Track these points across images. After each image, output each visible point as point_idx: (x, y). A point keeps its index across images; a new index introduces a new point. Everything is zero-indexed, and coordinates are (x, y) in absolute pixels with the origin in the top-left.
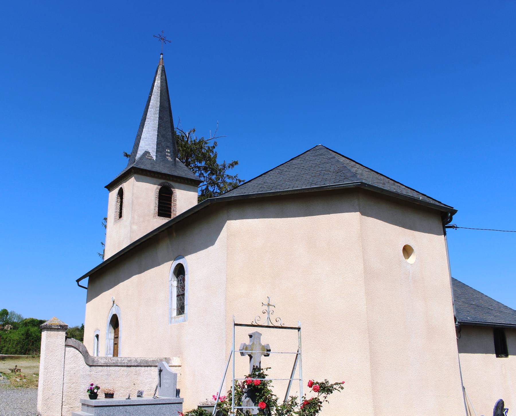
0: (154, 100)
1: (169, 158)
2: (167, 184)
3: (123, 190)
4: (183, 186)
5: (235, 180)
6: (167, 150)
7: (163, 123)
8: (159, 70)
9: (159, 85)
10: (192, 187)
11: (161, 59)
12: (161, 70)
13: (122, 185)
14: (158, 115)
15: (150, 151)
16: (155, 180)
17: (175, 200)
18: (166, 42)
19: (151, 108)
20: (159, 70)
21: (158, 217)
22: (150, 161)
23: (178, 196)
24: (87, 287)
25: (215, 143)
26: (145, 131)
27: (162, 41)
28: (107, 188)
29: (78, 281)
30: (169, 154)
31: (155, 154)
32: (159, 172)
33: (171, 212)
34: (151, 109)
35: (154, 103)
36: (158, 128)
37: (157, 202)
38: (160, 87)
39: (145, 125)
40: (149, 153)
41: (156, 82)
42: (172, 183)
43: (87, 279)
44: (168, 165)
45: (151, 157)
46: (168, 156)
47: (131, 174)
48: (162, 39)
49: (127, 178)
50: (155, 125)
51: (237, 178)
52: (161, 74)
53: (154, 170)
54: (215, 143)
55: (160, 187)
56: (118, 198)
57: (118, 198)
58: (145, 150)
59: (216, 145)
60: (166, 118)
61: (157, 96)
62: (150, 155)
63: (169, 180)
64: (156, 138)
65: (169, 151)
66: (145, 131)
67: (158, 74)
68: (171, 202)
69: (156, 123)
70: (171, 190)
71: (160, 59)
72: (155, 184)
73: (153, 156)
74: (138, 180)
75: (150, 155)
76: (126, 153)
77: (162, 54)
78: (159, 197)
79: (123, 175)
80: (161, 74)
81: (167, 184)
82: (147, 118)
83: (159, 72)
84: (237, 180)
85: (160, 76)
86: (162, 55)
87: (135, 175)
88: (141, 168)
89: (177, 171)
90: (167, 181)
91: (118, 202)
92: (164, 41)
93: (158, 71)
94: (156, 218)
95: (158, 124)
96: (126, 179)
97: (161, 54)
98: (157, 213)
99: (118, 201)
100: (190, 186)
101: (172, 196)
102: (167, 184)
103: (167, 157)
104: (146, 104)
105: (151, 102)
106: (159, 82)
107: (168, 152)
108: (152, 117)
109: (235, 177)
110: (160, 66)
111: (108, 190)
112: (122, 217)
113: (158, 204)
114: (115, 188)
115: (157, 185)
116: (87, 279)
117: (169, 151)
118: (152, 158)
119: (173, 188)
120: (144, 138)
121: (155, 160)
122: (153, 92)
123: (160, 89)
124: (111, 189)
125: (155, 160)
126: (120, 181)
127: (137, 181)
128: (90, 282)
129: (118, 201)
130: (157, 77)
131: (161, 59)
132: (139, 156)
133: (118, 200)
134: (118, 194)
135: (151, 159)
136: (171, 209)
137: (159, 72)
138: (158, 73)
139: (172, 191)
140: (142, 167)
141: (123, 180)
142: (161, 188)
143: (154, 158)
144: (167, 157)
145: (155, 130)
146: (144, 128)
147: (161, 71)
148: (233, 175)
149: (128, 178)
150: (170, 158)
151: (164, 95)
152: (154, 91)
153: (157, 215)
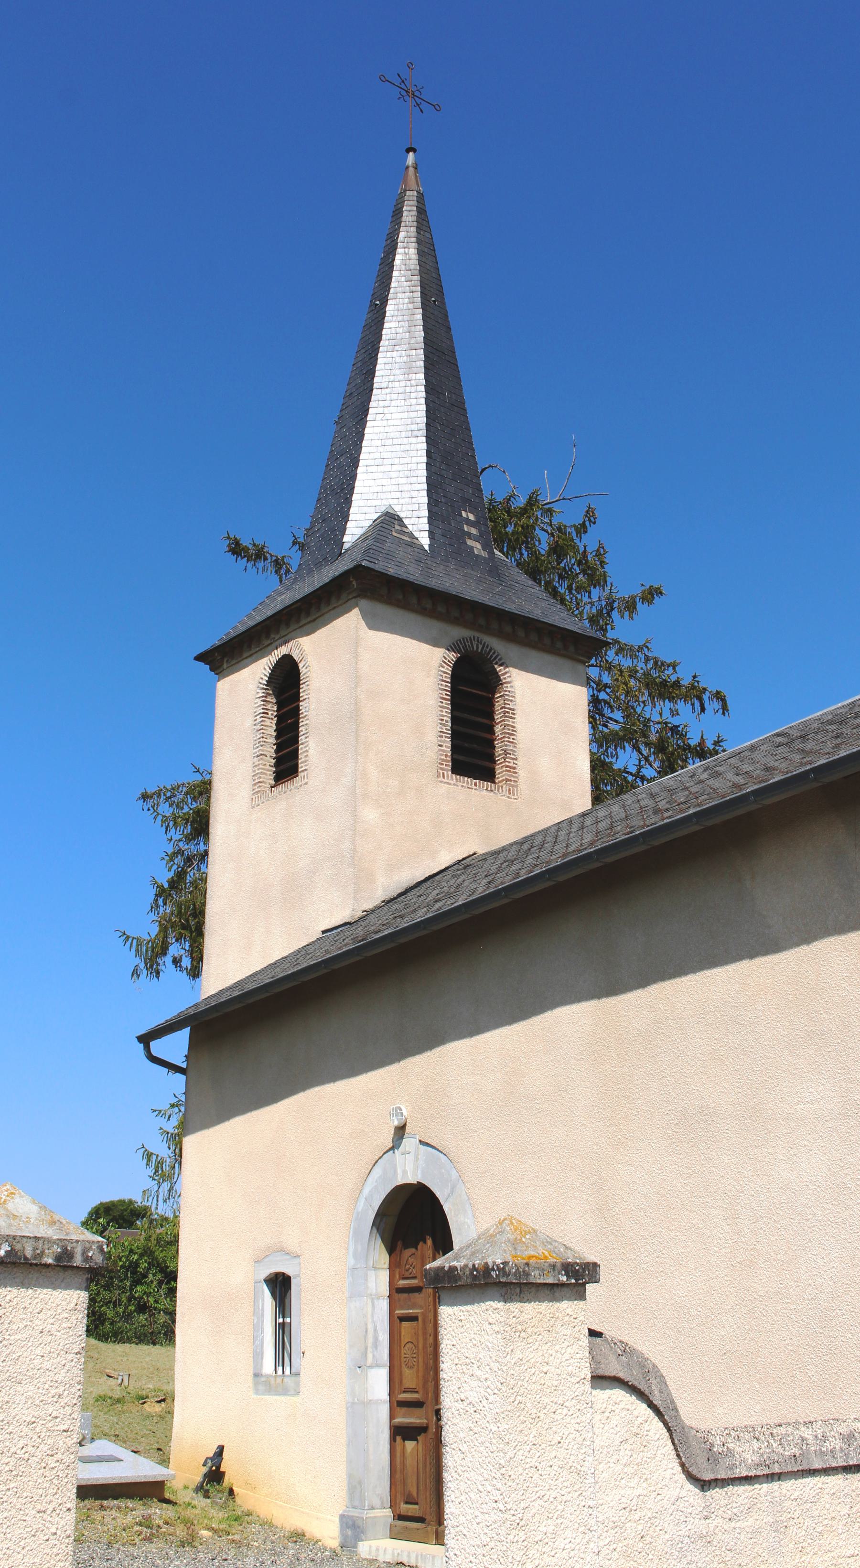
0: (400, 318)
1: (477, 547)
2: (477, 646)
3: (301, 665)
4: (535, 656)
5: (643, 660)
6: (464, 514)
7: (442, 409)
8: (409, 208)
9: (414, 263)
10: (565, 664)
11: (411, 170)
12: (415, 208)
13: (290, 644)
14: (422, 376)
15: (402, 515)
16: (435, 627)
17: (509, 713)
18: (424, 106)
19: (390, 348)
20: (409, 208)
21: (452, 779)
22: (410, 549)
23: (518, 699)
24: (184, 1065)
25: (590, 515)
26: (375, 437)
27: (411, 101)
28: (206, 664)
29: (146, 1039)
30: (474, 531)
31: (427, 527)
32: (454, 593)
33: (494, 762)
34: (389, 354)
35: (400, 330)
36: (427, 424)
37: (447, 718)
38: (417, 272)
39: (371, 411)
40: (400, 520)
41: (399, 251)
42: (497, 645)
43: (184, 1034)
44: (475, 573)
45: (411, 535)
46: (469, 535)
47: (344, 596)
48: (409, 93)
49: (319, 614)
50: (413, 415)
51: (650, 654)
52: (417, 222)
53: (433, 583)
54: (590, 515)
55: (453, 656)
56: (269, 699)
57: (269, 699)
58: (383, 509)
59: (590, 521)
60: (450, 392)
61: (411, 306)
62: (407, 528)
63: (487, 630)
64: (425, 465)
65: (471, 517)
66: (375, 437)
67: (403, 224)
68: (494, 719)
69: (417, 408)
70: (495, 669)
71: (407, 167)
72: (435, 643)
73: (416, 534)
74: (373, 625)
75: (404, 529)
76: (236, 539)
77: (414, 150)
78: (452, 696)
79: (299, 604)
80: (415, 224)
81: (477, 646)
82: (375, 386)
83: (409, 216)
84: (647, 659)
85: (414, 229)
86: (411, 154)
87: (363, 602)
88: (389, 573)
89: (514, 598)
90: (477, 634)
91: (270, 716)
92: (419, 101)
93: (405, 214)
94: (446, 780)
95: (427, 411)
96: (314, 620)
97: (408, 150)
98: (449, 759)
99: (270, 713)
100: (561, 661)
101: (494, 695)
102: (480, 647)
103: (470, 542)
104: (360, 336)
105: (386, 325)
106: (413, 252)
107: (468, 522)
108: (397, 384)
109: (640, 649)
110: (408, 193)
111: (212, 670)
112: (301, 775)
113: (450, 724)
114: (249, 659)
115: (443, 650)
116: (184, 1034)
117: (471, 517)
118: (415, 541)
119: (501, 665)
120: (372, 462)
121: (427, 548)
122: (392, 291)
123: (417, 278)
124: (225, 666)
125: (427, 548)
126: (278, 632)
127: (371, 627)
128: (194, 1044)
129: (270, 713)
130: (402, 235)
131: (411, 170)
132: (359, 532)
133: (269, 706)
134: (269, 683)
135: (412, 543)
136: (494, 747)
137: (409, 216)
138: (404, 219)
139: (499, 677)
140: (391, 570)
141: (292, 627)
142: (458, 660)
143: (425, 540)
144: (470, 542)
145: (415, 433)
146: (368, 425)
147: (415, 213)
148: (637, 642)
149: (327, 616)
150: (479, 546)
151: (434, 301)
152: (393, 285)
153: (447, 771)
